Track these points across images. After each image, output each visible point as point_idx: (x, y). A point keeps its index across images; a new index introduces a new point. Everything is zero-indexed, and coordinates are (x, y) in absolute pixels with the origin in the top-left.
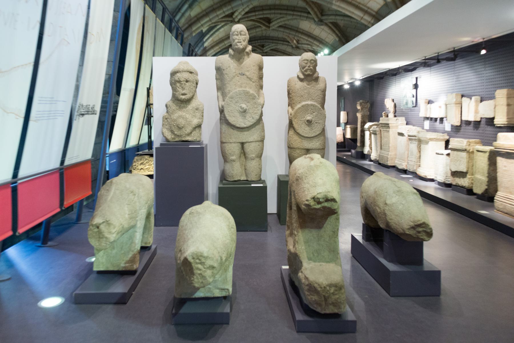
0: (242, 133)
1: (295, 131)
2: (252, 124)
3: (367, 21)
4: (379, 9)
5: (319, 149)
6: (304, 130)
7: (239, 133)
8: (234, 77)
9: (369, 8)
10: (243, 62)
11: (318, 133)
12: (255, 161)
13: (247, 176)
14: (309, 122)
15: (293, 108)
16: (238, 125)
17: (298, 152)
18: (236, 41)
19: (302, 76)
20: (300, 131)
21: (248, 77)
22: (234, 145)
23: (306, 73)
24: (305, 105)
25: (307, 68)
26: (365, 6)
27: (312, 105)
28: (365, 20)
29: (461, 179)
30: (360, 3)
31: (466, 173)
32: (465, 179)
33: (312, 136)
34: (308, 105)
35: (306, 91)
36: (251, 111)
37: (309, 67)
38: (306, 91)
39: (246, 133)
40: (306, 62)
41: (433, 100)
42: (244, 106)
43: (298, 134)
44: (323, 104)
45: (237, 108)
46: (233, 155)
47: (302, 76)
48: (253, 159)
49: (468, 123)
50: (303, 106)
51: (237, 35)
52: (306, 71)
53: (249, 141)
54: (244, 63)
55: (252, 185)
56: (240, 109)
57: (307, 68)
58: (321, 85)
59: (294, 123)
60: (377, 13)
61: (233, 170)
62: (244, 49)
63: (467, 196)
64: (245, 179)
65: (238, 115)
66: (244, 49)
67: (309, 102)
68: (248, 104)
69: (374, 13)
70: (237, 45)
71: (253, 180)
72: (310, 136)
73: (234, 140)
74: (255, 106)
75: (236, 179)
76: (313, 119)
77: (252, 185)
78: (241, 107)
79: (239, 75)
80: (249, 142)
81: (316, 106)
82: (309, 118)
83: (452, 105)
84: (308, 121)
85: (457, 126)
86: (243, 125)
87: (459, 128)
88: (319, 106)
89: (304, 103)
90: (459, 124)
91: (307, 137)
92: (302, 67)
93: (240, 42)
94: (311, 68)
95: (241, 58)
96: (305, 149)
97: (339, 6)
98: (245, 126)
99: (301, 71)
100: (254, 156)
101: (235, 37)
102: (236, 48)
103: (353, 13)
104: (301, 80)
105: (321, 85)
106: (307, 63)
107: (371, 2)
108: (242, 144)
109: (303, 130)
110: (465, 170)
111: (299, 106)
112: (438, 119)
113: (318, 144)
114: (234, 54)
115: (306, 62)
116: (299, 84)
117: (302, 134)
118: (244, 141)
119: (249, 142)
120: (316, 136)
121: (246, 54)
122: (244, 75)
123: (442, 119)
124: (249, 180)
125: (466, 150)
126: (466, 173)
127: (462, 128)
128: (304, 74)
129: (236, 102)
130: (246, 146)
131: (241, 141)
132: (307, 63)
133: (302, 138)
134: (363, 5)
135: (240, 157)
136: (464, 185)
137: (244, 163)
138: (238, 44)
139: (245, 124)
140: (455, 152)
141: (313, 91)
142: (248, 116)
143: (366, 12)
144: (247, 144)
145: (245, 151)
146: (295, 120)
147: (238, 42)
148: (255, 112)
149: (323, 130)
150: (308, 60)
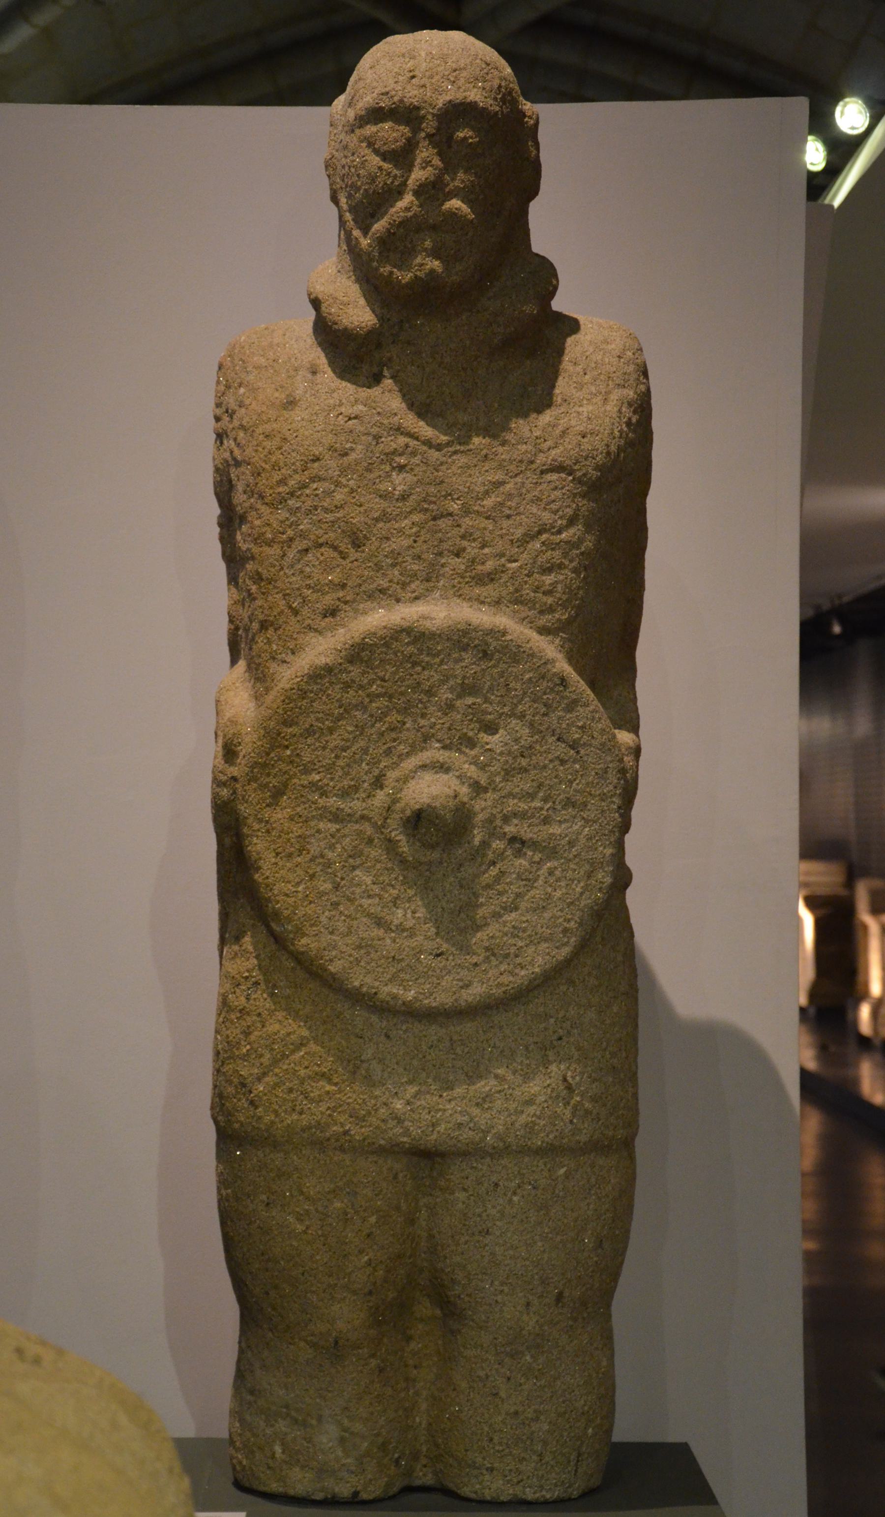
1: (278, 939)
5: (550, 1151)
6: (371, 927)
11: (538, 959)
14: (437, 834)
15: (259, 675)
19: (358, 314)
27: (462, 639)
33: (476, 992)
34: (417, 636)
35: (400, 482)
37: (432, 192)
38: (400, 482)
40: (390, 133)
44: (606, 626)
47: (358, 314)
50: (359, 653)
52: (397, 244)
58: (581, 412)
59: (257, 845)
67: (438, 612)
72: (442, 999)
76: (483, 806)
81: (516, 654)
82: (428, 789)
84: (418, 820)
88: (550, 650)
89: (377, 618)
91: (412, 1013)
92: (363, 205)
94: (455, 203)
96: (392, 1150)
99: (352, 248)
105: (581, 412)
106: (402, 157)
111: (321, 649)
113: (535, 1087)
115: (390, 133)
117: (357, 980)
128: (374, 286)
132: (402, 157)
133: (359, 1016)
141: (479, 479)
146: (279, 815)
149: (608, 926)
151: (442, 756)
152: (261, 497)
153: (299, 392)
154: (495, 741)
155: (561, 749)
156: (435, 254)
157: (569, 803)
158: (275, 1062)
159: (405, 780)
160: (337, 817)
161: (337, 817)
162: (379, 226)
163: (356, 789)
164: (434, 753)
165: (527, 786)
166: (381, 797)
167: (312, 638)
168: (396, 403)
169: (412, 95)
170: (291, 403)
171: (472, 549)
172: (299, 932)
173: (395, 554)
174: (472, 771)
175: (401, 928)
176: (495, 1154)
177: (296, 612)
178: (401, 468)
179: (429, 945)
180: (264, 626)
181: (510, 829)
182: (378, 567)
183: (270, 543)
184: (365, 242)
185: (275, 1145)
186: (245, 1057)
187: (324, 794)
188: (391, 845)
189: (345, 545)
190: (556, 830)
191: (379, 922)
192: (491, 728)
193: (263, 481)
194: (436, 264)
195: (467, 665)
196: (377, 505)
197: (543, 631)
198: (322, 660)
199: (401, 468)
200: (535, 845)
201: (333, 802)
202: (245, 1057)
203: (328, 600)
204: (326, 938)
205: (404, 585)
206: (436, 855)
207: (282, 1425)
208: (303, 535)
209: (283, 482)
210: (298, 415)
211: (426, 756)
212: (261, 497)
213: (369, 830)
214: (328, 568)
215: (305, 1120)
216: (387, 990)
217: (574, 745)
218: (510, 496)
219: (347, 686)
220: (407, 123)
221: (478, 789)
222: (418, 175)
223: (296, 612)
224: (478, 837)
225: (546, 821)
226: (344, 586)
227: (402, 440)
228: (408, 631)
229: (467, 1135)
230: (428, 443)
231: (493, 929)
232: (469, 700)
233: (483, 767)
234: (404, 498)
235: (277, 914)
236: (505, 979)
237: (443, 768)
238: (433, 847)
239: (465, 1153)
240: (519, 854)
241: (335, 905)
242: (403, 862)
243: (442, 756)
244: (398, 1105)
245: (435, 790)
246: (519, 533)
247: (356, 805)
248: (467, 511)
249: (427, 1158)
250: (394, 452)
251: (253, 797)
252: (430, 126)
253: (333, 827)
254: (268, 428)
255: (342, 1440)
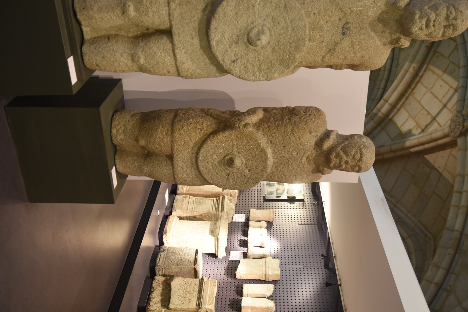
0: (195, 33)
1: (209, 136)
2: (220, 59)
3: (382, 107)
4: (395, 124)
7: (196, 25)
8: (341, 10)
9: (399, 110)
10: (375, 32)
12: (130, 63)
13: (94, 40)
16: (214, 24)
17: (165, 140)
18: (433, 16)
20: (209, 145)
21: (336, 44)
22: (164, 11)
23: (333, 156)
24: (266, 156)
25: (345, 158)
26: (402, 106)
27: (265, 167)
28: (383, 105)
29: (160, 297)
30: (407, 99)
31: (168, 308)
32: (159, 305)
33: (201, 168)
34: (266, 160)
36: (251, 56)
39: (196, 41)
40: (358, 156)
41: (272, 230)
42: (264, 39)
43: (203, 142)
45: (259, 21)
46: (137, 10)
48: (133, 60)
49: (240, 293)
50: (263, 151)
51: (447, 18)
52: (338, 156)
53: (177, 51)
54: (373, 34)
55: (71, 61)
56: (255, 31)
57: (345, 158)
60: (391, 120)
61: (100, 10)
62: (406, 32)
63: (137, 307)
64: (86, 37)
65: (243, 23)
66: (406, 32)
68: (269, 49)
69: (390, 117)
70: (421, 18)
71: (86, 58)
72: (200, 163)
73: (176, 14)
74: (263, 67)
75: (80, 17)
76: (235, 170)
77: (71, 61)
78: (261, 32)
79: (343, 22)
80: (173, 51)
82: (238, 162)
83: (264, 269)
85: (235, 275)
86: (215, 37)
87: (233, 276)
89: (269, 151)
90: (238, 276)
91: (197, 158)
93: (427, 26)
95: (385, 25)
97: (407, 71)
98: (214, 43)
100: (142, 61)
101: (443, 14)
102: (413, 14)
103: (395, 90)
104: (319, 143)
107: (406, 114)
108: (168, 33)
109: (211, 152)
110: (171, 306)
111: (263, 141)
112: (246, 238)
113: (185, 176)
114: (398, 8)
115: (358, 156)
116: (309, 140)
117: (202, 150)
118: (176, 38)
119: (173, 51)
120: (201, 174)
121: (394, 36)
122: (344, 34)
123: (244, 244)
124: (85, 49)
125: (200, 308)
126: (168, 308)
127: (233, 281)
128: (331, 150)
129: (274, 20)
130: (164, 41)
131: (175, 30)
133: (196, 149)
134: (404, 103)
135: (137, 26)
136: (151, 304)
137: (123, 33)
138: (424, 22)
139: (217, 43)
140: (197, 289)
142: (240, 49)
143: (394, 106)
144: (169, 46)
145: (153, 39)
146: (233, 136)
147: (428, 21)
148: (250, 67)
150: (360, 160)
151: (244, 163)
152: (293, 127)
153: (312, 134)
154: (247, 171)
155: (245, 181)
156: (336, 163)
157: (236, 183)
158: (187, 134)
159: (240, 157)
160: (233, 146)
161: (233, 146)
162: (342, 153)
163: (238, 149)
164: (245, 162)
165: (239, 176)
166: (236, 153)
167: (266, 139)
168: (309, 153)
169: (364, 160)
170: (310, 133)
171: (282, 166)
172: (211, 141)
173: (281, 153)
174: (241, 168)
175: (212, 157)
176: (173, 170)
177: (271, 135)
178: (297, 154)
179: (209, 161)
180: (269, 127)
181: (231, 173)
182: (279, 151)
183: (284, 129)
184: (339, 149)
185: (172, 133)
186: (188, 128)
187: (237, 144)
188: (227, 155)
189: (283, 145)
190: (231, 181)
191: (213, 153)
192: (249, 171)
193: (296, 127)
194: (334, 163)
195: (261, 167)
196: (291, 150)
197: (267, 177)
198: (262, 144)
199: (297, 154)
200: (228, 177)
201: (235, 145)
202: (188, 128)
203: (274, 142)
204: (210, 145)
205: (276, 155)
206: (226, 162)
207: (123, 128)
208: (286, 136)
209: (296, 133)
210: (308, 135)
211: (244, 161)
212: (293, 127)
213: (230, 152)
214: (280, 141)
215: (177, 139)
216: (201, 155)
217: (246, 183)
218: (291, 171)
219: (257, 148)
220: (359, 159)
221: (239, 169)
222: (350, 161)
223: (271, 135)
224: (229, 169)
225: (233, 179)
226: (276, 144)
227: (302, 154)
228: (267, 158)
229: (176, 166)
230: (302, 158)
231: (213, 171)
232: (254, 167)
233: (242, 169)
234: (292, 155)
235: (214, 136)
236: (204, 173)
237: (242, 163)
238: (227, 162)
239: (172, 164)
240: (227, 175)
241: (216, 146)
242: (224, 157)
243: (244, 163)
244: (180, 155)
245: (238, 164)
246: (285, 173)
247: (235, 149)
248: (289, 164)
249: (171, 158)
250: (300, 153)
251: (236, 132)
252: (358, 164)
253: (231, 145)
254: (306, 128)
255: (122, 139)
